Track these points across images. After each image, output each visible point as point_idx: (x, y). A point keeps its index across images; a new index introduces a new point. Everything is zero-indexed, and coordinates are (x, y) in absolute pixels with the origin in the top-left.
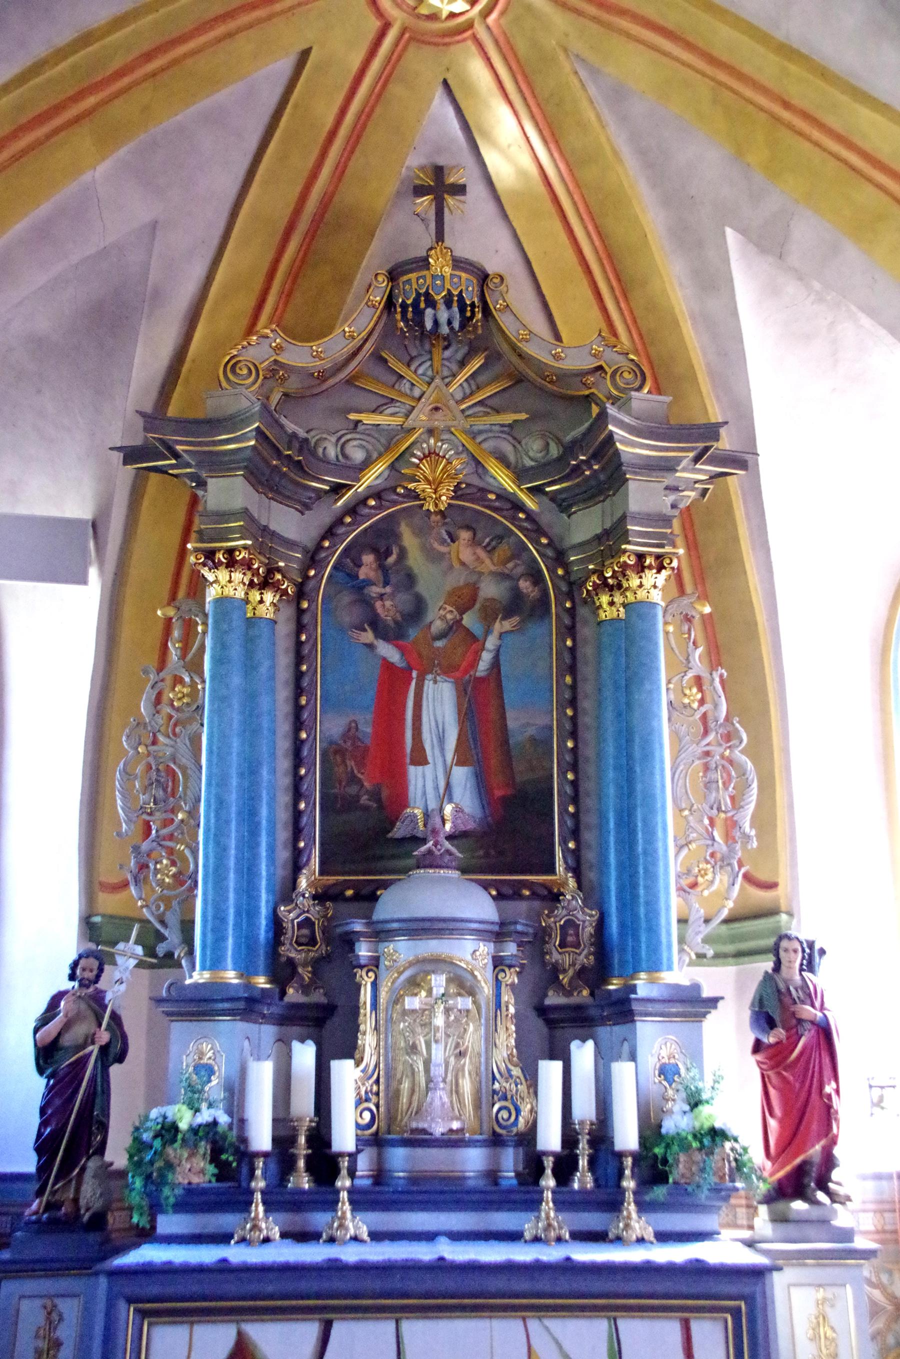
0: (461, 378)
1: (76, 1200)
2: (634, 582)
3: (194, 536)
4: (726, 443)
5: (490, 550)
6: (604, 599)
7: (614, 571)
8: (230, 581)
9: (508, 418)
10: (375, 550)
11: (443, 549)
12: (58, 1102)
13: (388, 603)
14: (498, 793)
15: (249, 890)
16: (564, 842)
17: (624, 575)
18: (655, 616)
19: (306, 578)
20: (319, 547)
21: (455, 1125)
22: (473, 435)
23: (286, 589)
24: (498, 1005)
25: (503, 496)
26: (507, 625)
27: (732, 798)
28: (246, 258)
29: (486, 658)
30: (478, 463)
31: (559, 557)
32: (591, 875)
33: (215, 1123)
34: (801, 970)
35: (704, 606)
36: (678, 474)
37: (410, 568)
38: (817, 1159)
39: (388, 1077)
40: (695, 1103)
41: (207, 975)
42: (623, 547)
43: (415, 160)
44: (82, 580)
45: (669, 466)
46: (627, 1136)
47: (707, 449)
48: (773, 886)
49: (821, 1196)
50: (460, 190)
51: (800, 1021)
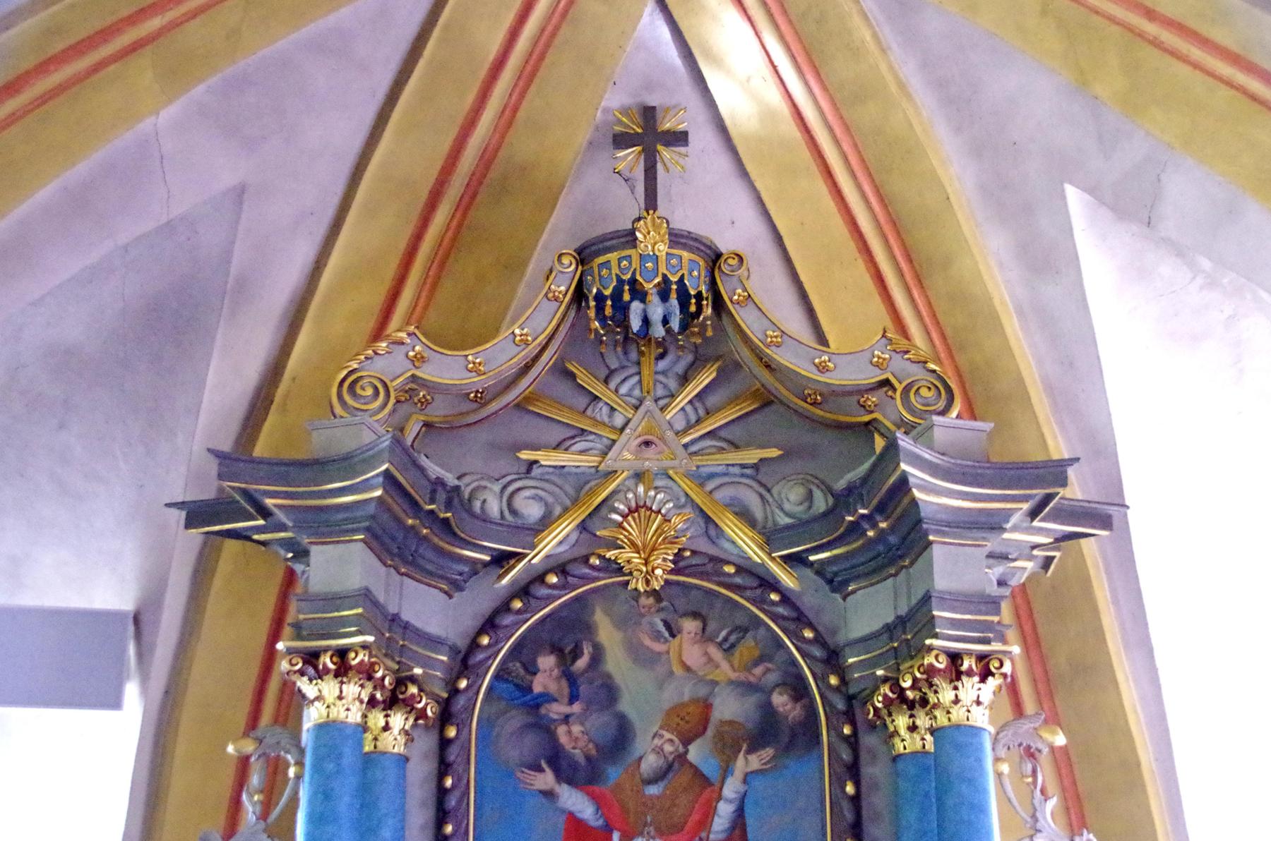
0: (683, 399)
2: (946, 695)
3: (287, 630)
4: (1076, 490)
5: (728, 649)
6: (902, 721)
7: (915, 680)
8: (340, 698)
10: (557, 650)
11: (658, 647)
13: (576, 729)
17: (931, 685)
18: (980, 748)
19: (455, 692)
20: (474, 645)
22: (701, 480)
23: (424, 709)
26: (755, 762)
28: (374, 234)
29: (724, 812)
30: (708, 519)
31: (832, 659)
35: (1054, 733)
36: (1006, 536)
37: (609, 676)
42: (928, 642)
43: (615, 100)
44: (115, 703)
45: (992, 524)
47: (1048, 498)
50: (680, 138)
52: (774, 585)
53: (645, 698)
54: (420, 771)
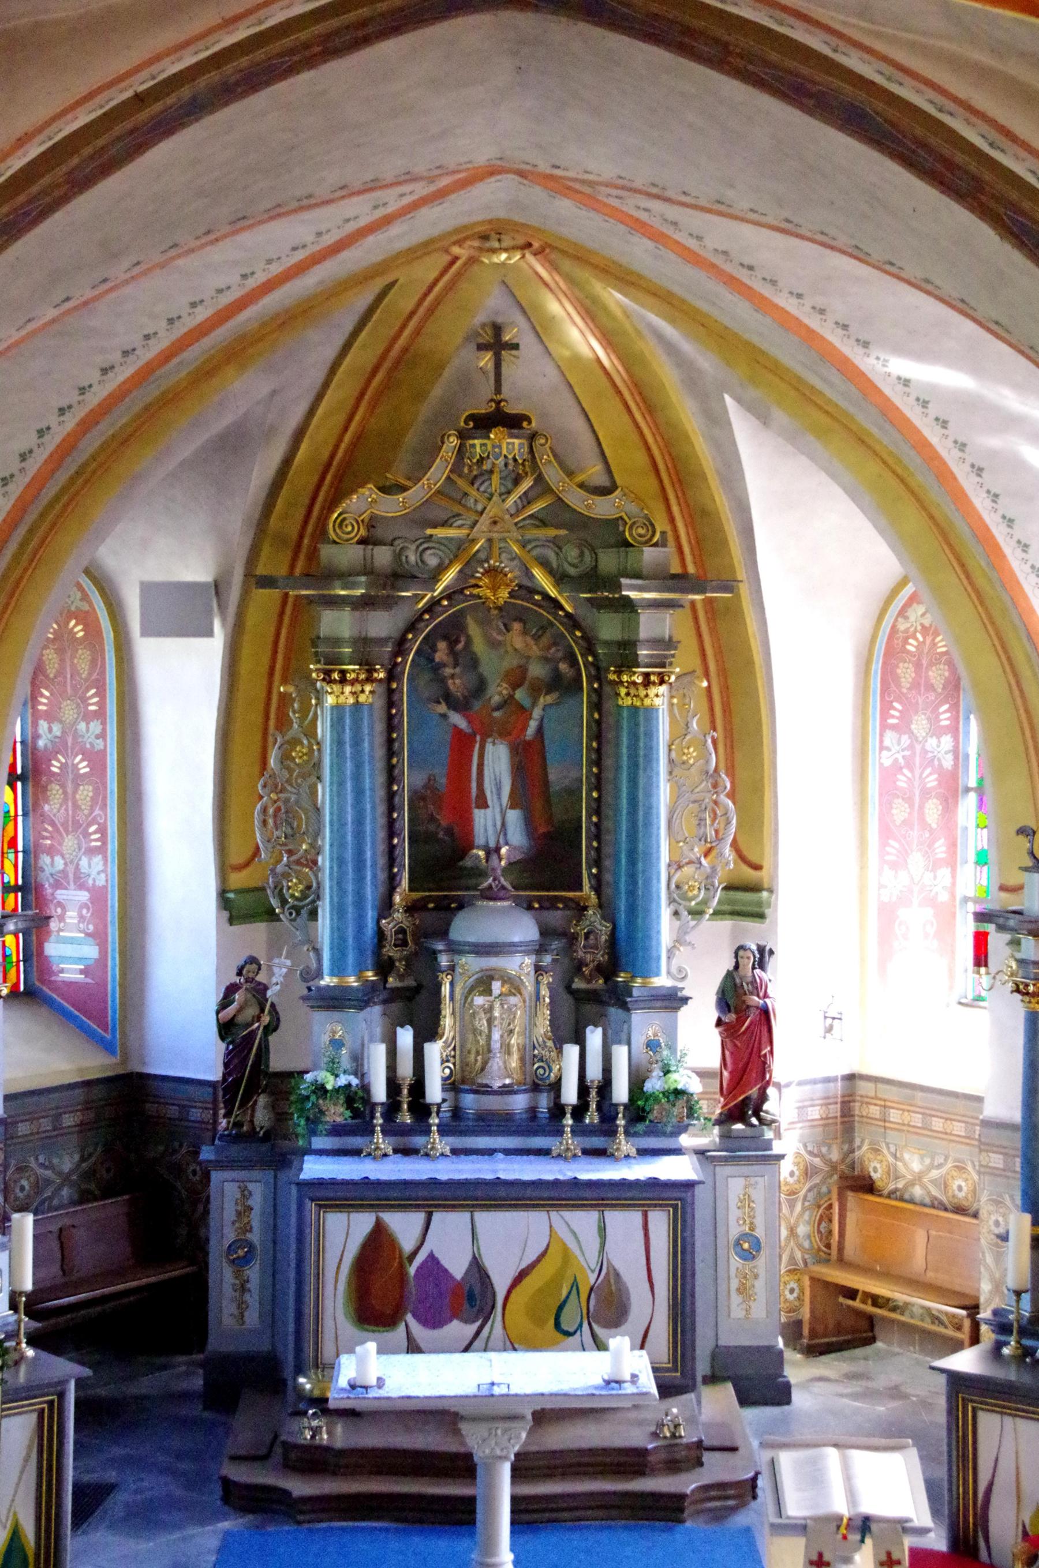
0: (513, 498)
1: (252, 1121)
5: (537, 638)
9: (552, 532)
10: (445, 638)
12: (236, 1061)
13: (457, 681)
14: (542, 830)
15: (360, 918)
16: (589, 868)
19: (395, 665)
21: (507, 1081)
22: (523, 545)
24: (538, 998)
25: (546, 596)
26: (549, 699)
27: (717, 832)
29: (533, 725)
31: (589, 644)
32: (607, 891)
33: (349, 1085)
34: (754, 968)
37: (474, 653)
38: (755, 1096)
39: (462, 1046)
40: (667, 1072)
41: (335, 980)
44: (210, 633)
46: (621, 1093)
48: (757, 867)
49: (754, 1121)
51: (748, 1007)
52: (562, 608)
53: (494, 665)
54: (379, 714)
